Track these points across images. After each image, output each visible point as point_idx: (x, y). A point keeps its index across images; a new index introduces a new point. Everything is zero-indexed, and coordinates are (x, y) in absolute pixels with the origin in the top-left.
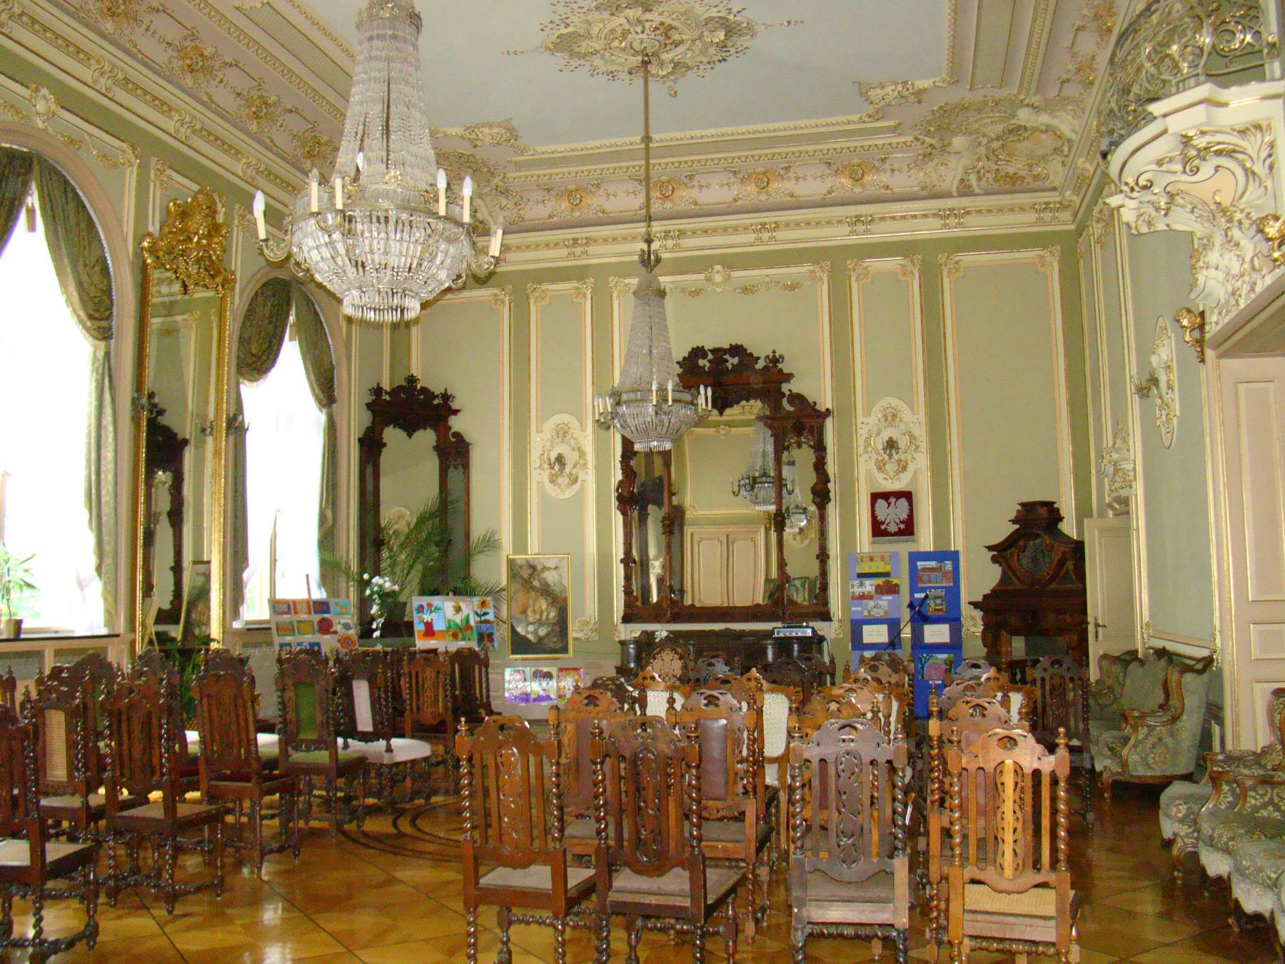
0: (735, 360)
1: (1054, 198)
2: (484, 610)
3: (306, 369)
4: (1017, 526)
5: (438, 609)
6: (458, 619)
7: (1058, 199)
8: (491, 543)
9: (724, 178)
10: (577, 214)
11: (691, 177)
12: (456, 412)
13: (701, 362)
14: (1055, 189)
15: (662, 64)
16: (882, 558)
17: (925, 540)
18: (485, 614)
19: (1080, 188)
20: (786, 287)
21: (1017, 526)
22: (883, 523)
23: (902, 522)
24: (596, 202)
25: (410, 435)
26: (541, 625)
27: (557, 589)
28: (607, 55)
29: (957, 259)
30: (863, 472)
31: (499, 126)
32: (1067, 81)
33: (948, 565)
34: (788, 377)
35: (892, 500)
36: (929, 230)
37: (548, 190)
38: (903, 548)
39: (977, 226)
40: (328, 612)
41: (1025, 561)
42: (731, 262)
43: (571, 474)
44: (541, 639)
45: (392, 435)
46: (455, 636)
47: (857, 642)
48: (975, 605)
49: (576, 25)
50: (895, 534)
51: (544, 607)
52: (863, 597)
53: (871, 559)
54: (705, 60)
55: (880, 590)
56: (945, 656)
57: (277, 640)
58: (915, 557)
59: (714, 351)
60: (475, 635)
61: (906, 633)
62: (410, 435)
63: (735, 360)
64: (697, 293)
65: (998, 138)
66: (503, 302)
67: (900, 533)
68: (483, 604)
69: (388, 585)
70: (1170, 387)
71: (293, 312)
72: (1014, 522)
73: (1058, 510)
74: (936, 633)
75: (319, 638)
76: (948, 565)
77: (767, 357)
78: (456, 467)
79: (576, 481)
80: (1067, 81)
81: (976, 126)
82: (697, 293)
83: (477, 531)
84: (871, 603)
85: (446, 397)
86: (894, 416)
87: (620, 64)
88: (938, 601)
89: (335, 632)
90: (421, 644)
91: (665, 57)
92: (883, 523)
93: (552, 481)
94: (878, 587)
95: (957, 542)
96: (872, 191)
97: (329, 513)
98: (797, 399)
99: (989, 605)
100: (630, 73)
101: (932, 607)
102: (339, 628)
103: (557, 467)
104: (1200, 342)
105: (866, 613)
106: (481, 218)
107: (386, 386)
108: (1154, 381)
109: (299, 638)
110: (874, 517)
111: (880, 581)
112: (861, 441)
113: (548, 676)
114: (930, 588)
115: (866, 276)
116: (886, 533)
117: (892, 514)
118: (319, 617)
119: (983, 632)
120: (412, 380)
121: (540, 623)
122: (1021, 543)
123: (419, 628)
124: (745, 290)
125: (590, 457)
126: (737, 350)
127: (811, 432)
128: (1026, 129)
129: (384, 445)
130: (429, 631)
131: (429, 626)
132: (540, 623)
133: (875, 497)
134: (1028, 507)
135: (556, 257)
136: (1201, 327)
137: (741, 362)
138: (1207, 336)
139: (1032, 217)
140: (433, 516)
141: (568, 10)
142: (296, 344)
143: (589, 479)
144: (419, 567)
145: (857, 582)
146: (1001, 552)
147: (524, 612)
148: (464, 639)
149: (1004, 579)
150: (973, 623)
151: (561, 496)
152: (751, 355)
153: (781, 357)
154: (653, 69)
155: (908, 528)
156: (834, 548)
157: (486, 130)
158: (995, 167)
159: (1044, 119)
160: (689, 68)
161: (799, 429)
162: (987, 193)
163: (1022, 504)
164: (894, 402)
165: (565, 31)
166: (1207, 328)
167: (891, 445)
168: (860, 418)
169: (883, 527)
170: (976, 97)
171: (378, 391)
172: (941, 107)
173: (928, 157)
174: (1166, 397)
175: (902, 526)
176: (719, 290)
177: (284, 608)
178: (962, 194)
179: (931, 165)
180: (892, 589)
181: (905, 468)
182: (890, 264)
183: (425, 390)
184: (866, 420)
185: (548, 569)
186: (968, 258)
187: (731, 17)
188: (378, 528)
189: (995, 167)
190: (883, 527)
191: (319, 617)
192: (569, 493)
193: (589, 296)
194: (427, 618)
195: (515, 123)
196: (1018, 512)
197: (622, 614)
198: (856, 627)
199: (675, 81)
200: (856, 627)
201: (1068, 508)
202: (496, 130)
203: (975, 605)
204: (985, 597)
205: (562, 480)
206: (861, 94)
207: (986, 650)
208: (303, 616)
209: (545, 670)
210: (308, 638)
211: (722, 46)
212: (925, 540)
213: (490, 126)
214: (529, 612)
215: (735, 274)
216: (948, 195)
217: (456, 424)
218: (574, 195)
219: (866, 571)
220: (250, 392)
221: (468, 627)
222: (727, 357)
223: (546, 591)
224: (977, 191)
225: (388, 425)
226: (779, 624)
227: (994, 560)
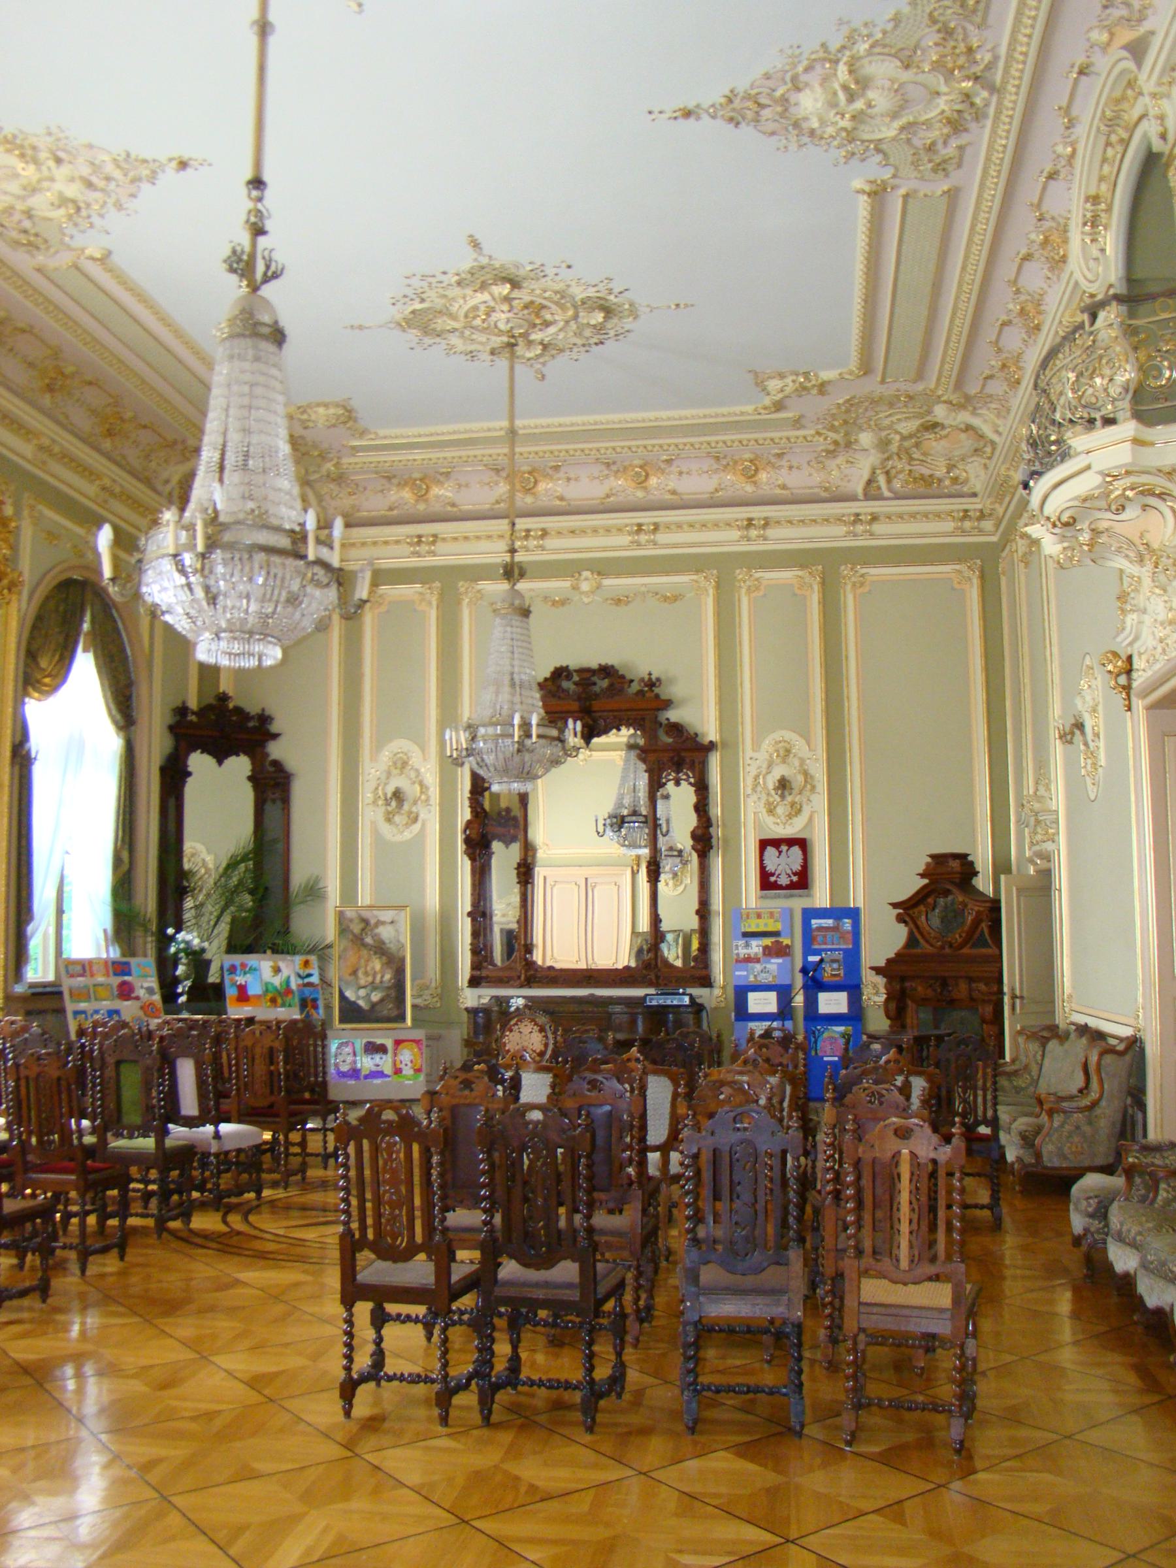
0: (605, 683)
1: (974, 505)
2: (308, 971)
4: (926, 881)
5: (253, 970)
6: (277, 981)
7: (980, 506)
8: (314, 892)
9: (597, 470)
10: (421, 507)
11: (556, 468)
12: (275, 736)
13: (565, 684)
14: (975, 495)
15: (530, 343)
16: (772, 915)
17: (821, 895)
18: (309, 975)
19: (1004, 496)
20: (666, 599)
21: (926, 881)
22: (772, 875)
23: (795, 874)
24: (442, 492)
25: (220, 763)
26: (375, 989)
27: (392, 947)
28: (467, 333)
29: (864, 571)
30: (752, 817)
31: (337, 405)
32: (991, 377)
33: (847, 924)
34: (667, 704)
35: (784, 848)
36: (833, 536)
37: (389, 478)
38: (797, 903)
39: (887, 533)
40: (129, 974)
41: (935, 921)
42: (603, 568)
43: (410, 812)
44: (374, 1005)
45: (199, 762)
46: (273, 1001)
47: (742, 1013)
48: (878, 970)
49: (434, 300)
50: (788, 887)
51: (378, 966)
52: (748, 960)
53: (759, 916)
54: (579, 342)
55: (769, 952)
56: (841, 1029)
57: (70, 1007)
58: (809, 914)
59: (581, 671)
60: (297, 1000)
61: (799, 1000)
62: (220, 763)
63: (605, 683)
64: (563, 602)
65: (911, 436)
67: (792, 886)
68: (306, 963)
69: (196, 941)
70: (1097, 735)
71: (88, 618)
72: (922, 876)
73: (972, 863)
74: (832, 1003)
75: (119, 1004)
76: (847, 924)
77: (642, 680)
78: (274, 801)
79: (416, 820)
80: (991, 377)
81: (887, 422)
82: (563, 602)
83: (299, 877)
84: (758, 967)
85: (264, 719)
86: (788, 751)
87: (481, 343)
88: (835, 966)
89: (137, 998)
90: (236, 1012)
91: (536, 336)
92: (772, 875)
93: (389, 820)
94: (766, 948)
95: (857, 898)
96: (766, 491)
97: (125, 855)
98: (676, 729)
99: (890, 970)
100: (492, 353)
101: (829, 972)
102: (141, 993)
103: (394, 804)
104: (1127, 688)
105: (752, 978)
107: (193, 704)
108: (1080, 726)
109: (95, 1005)
110: (762, 868)
111: (768, 941)
112: (750, 781)
113: (382, 1049)
114: (826, 950)
115: (757, 588)
116: (776, 886)
117: (784, 864)
119: (887, 1000)
120: (223, 698)
122: (930, 900)
123: (231, 992)
124: (618, 602)
125: (434, 792)
126: (606, 671)
127: (692, 768)
128: (943, 427)
129: (189, 774)
130: (243, 995)
131: (242, 989)
132: (374, 987)
133: (764, 844)
134: (939, 860)
135: (399, 558)
136: (1129, 672)
137: (611, 685)
138: (1135, 685)
139: (950, 526)
140: (244, 858)
141: (425, 284)
142: (90, 657)
143: (431, 819)
144: (227, 918)
145: (741, 942)
146: (908, 910)
147: (354, 973)
148: (283, 1005)
149: (911, 942)
150: (875, 992)
151: (399, 838)
152: (623, 677)
153: (658, 680)
154: (519, 350)
155: (802, 881)
156: (717, 903)
157: (321, 410)
158: (908, 468)
159: (964, 417)
160: (561, 351)
161: (678, 766)
162: (898, 497)
163: (932, 856)
164: (789, 735)
165: (418, 306)
166: (1134, 675)
167: (783, 785)
168: (749, 753)
169: (772, 879)
170: (888, 391)
171: (182, 711)
172: (847, 401)
173: (831, 454)
174: (1091, 744)
175: (795, 879)
176: (586, 600)
177: (79, 969)
178: (867, 497)
179: (832, 464)
180: (780, 951)
181: (799, 811)
182: (786, 575)
183: (238, 710)
184: (755, 755)
185: (383, 923)
186: (877, 572)
187: (612, 297)
188: (182, 875)
189: (908, 468)
190: (772, 879)
192: (408, 835)
193: (434, 603)
194: (240, 979)
195: (354, 404)
196: (928, 864)
197: (467, 976)
198: (741, 992)
199: (544, 364)
200: (741, 992)
201: (983, 859)
202: (332, 411)
203: (878, 970)
204: (889, 961)
206: (757, 384)
207: (888, 1022)
208: (101, 979)
209: (379, 1041)
210: (107, 1004)
211: (599, 329)
212: (821, 895)
213: (326, 406)
214: (360, 974)
215: (607, 582)
216: (853, 498)
217: (275, 750)
218: (422, 482)
219: (753, 929)
221: (288, 991)
222: (595, 679)
223: (380, 949)
224: (887, 494)
225: (194, 750)
226: (652, 991)
227: (900, 919)
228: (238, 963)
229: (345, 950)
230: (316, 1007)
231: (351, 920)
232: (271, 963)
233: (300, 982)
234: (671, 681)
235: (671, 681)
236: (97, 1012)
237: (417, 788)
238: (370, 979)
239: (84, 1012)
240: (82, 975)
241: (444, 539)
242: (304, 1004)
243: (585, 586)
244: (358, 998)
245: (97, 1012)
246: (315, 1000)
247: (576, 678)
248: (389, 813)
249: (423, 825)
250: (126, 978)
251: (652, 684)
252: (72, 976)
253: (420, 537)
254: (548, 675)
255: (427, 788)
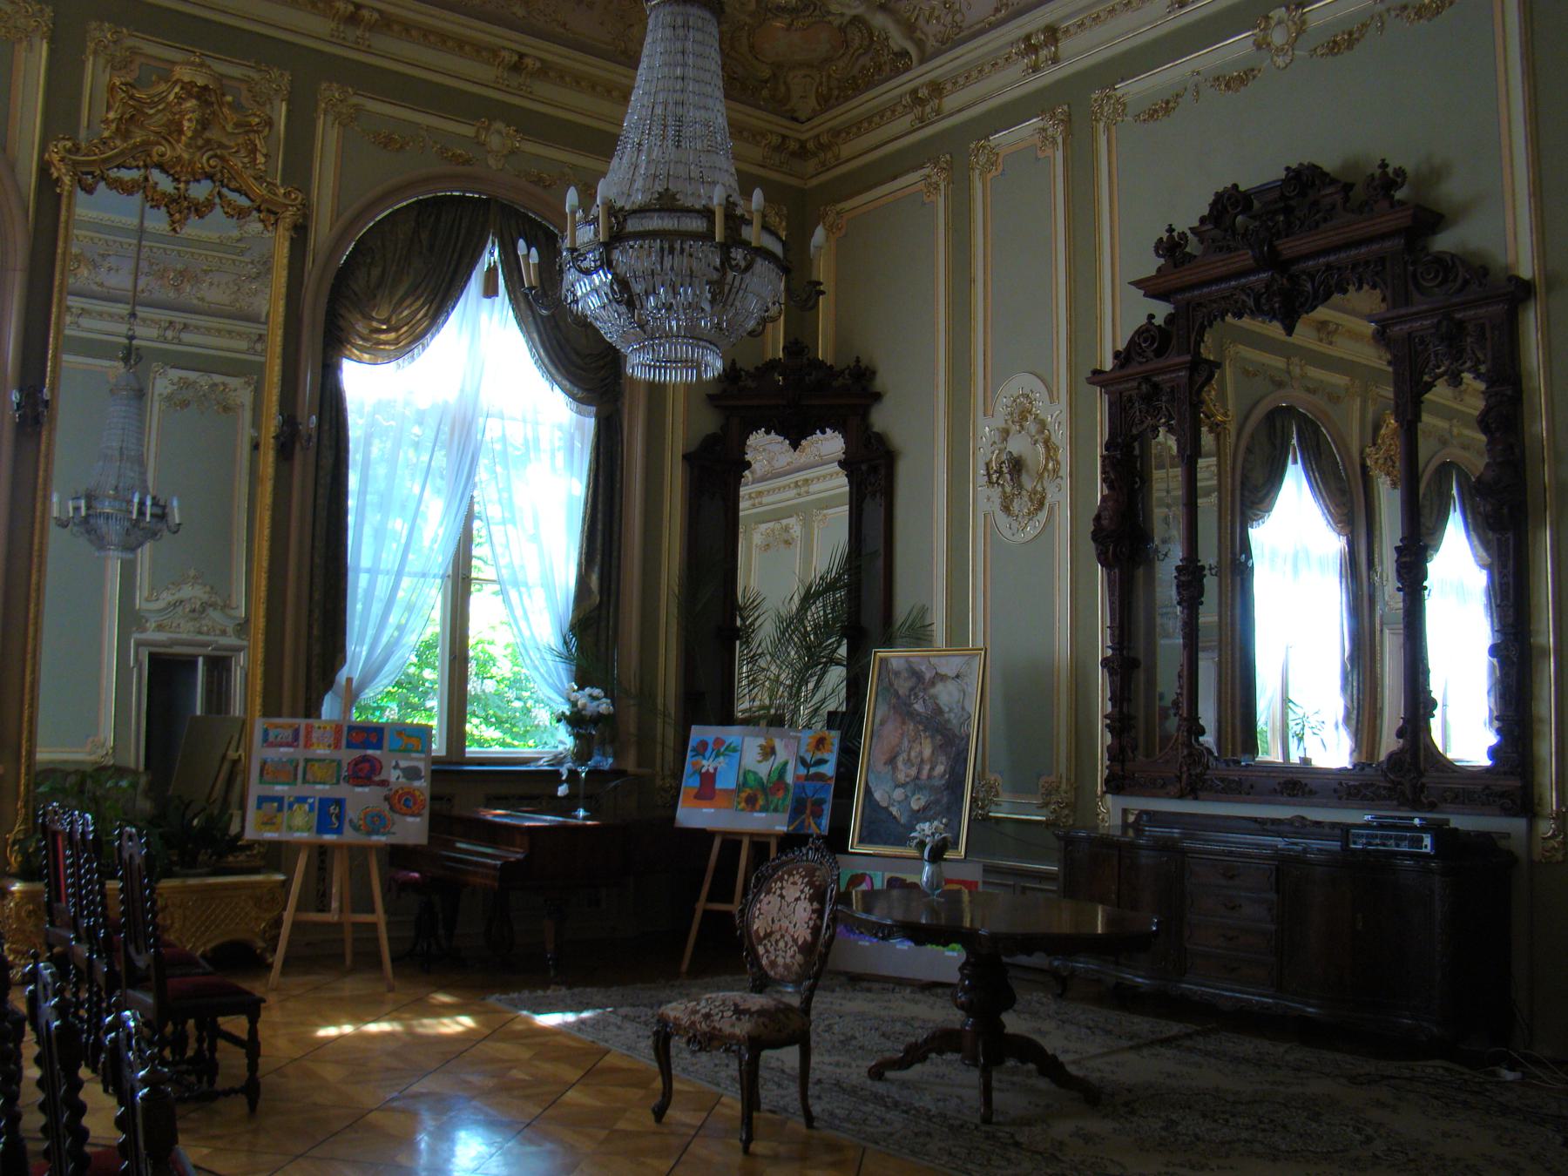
2: (819, 755)
3: (529, 339)
6: (763, 769)
12: (878, 397)
18: (822, 762)
25: (795, 445)
34: (1429, 220)
40: (379, 746)
43: (1035, 492)
45: (765, 449)
51: (927, 752)
59: (1261, 191)
60: (789, 801)
62: (795, 445)
66: (937, 188)
78: (874, 495)
79: (1041, 504)
89: (384, 783)
90: (692, 815)
93: (1006, 509)
102: (394, 776)
106: (896, 49)
109: (301, 789)
118: (357, 753)
121: (916, 784)
123: (690, 782)
125: (1064, 455)
129: (748, 465)
131: (708, 779)
132: (916, 784)
140: (831, 587)
143: (1060, 495)
147: (891, 761)
148: (764, 809)
152: (1333, 181)
153: (1400, 172)
161: (1453, 337)
176: (1280, 61)
185: (942, 678)
191: (357, 753)
193: (1060, 140)
194: (708, 765)
205: (1021, 505)
208: (321, 751)
210: (323, 790)
220: (364, 383)
225: (757, 429)
228: (710, 741)
229: (882, 723)
230: (817, 814)
231: (897, 674)
232: (762, 741)
233: (802, 771)
234: (1436, 174)
235: (1436, 174)
236: (301, 800)
237: (1041, 448)
238: (913, 772)
239: (280, 800)
240: (288, 745)
241: (1067, 31)
242: (798, 808)
243: (1278, 37)
244: (892, 802)
245: (301, 800)
246: (821, 802)
247: (1257, 204)
248: (1005, 496)
249: (1051, 509)
250: (370, 752)
251: (1387, 181)
252: (272, 745)
253: (1028, 38)
254: (1206, 212)
255: (1056, 449)
